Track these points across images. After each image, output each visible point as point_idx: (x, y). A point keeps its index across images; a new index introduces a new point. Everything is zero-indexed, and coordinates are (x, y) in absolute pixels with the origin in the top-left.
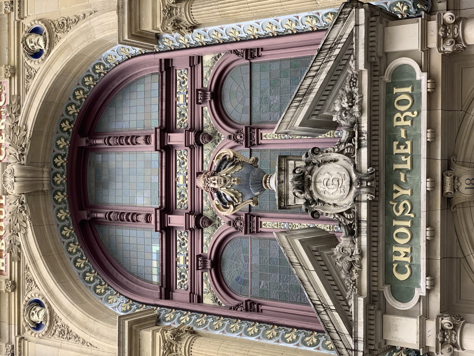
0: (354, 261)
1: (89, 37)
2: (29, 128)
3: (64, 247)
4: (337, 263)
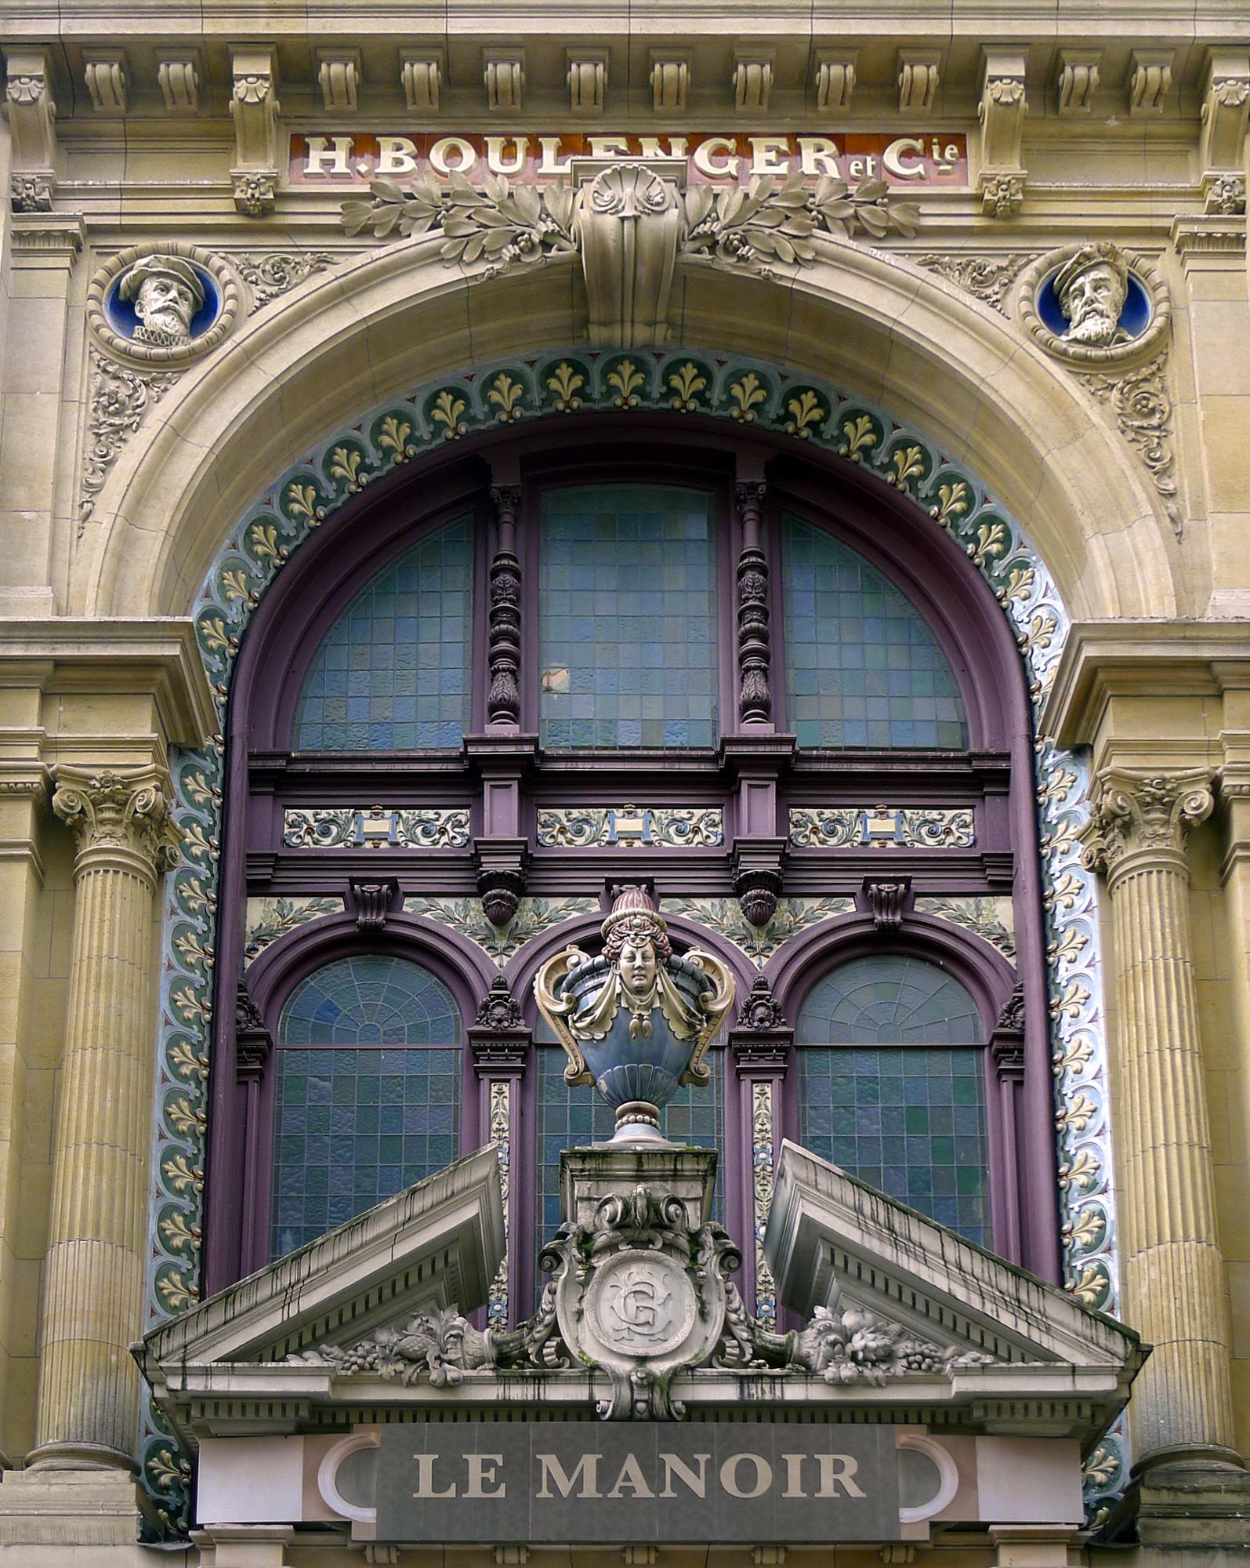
0: (426, 1366)
1: (1099, 513)
2: (804, 275)
3: (400, 403)
4: (419, 1321)
